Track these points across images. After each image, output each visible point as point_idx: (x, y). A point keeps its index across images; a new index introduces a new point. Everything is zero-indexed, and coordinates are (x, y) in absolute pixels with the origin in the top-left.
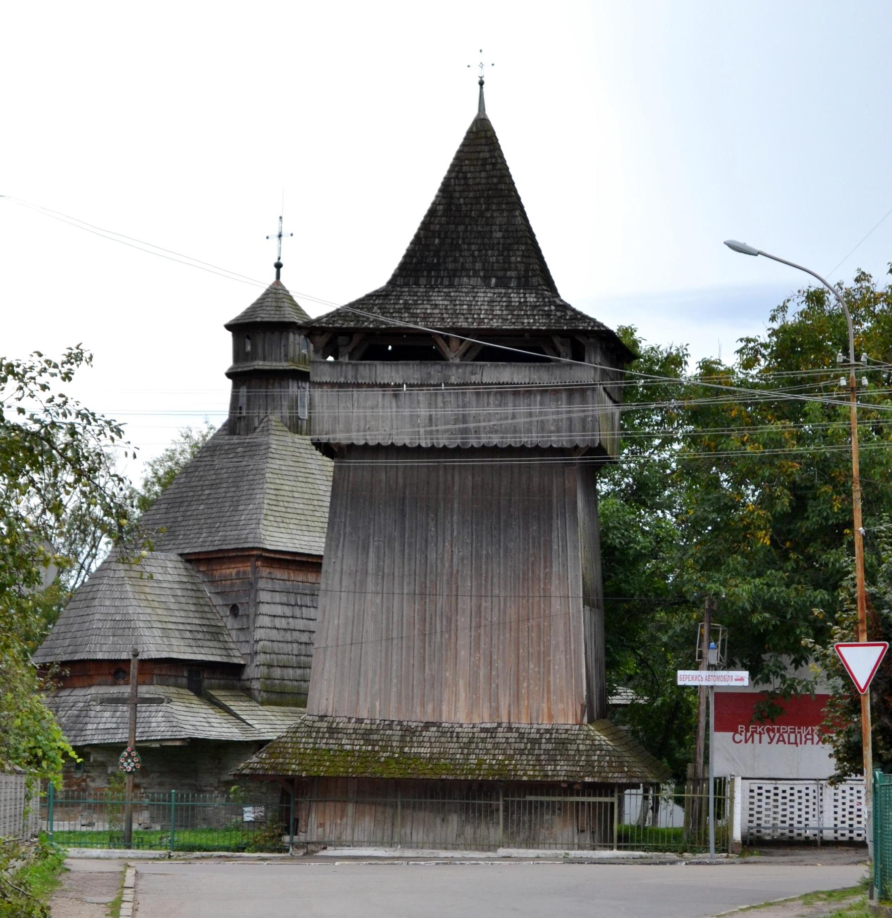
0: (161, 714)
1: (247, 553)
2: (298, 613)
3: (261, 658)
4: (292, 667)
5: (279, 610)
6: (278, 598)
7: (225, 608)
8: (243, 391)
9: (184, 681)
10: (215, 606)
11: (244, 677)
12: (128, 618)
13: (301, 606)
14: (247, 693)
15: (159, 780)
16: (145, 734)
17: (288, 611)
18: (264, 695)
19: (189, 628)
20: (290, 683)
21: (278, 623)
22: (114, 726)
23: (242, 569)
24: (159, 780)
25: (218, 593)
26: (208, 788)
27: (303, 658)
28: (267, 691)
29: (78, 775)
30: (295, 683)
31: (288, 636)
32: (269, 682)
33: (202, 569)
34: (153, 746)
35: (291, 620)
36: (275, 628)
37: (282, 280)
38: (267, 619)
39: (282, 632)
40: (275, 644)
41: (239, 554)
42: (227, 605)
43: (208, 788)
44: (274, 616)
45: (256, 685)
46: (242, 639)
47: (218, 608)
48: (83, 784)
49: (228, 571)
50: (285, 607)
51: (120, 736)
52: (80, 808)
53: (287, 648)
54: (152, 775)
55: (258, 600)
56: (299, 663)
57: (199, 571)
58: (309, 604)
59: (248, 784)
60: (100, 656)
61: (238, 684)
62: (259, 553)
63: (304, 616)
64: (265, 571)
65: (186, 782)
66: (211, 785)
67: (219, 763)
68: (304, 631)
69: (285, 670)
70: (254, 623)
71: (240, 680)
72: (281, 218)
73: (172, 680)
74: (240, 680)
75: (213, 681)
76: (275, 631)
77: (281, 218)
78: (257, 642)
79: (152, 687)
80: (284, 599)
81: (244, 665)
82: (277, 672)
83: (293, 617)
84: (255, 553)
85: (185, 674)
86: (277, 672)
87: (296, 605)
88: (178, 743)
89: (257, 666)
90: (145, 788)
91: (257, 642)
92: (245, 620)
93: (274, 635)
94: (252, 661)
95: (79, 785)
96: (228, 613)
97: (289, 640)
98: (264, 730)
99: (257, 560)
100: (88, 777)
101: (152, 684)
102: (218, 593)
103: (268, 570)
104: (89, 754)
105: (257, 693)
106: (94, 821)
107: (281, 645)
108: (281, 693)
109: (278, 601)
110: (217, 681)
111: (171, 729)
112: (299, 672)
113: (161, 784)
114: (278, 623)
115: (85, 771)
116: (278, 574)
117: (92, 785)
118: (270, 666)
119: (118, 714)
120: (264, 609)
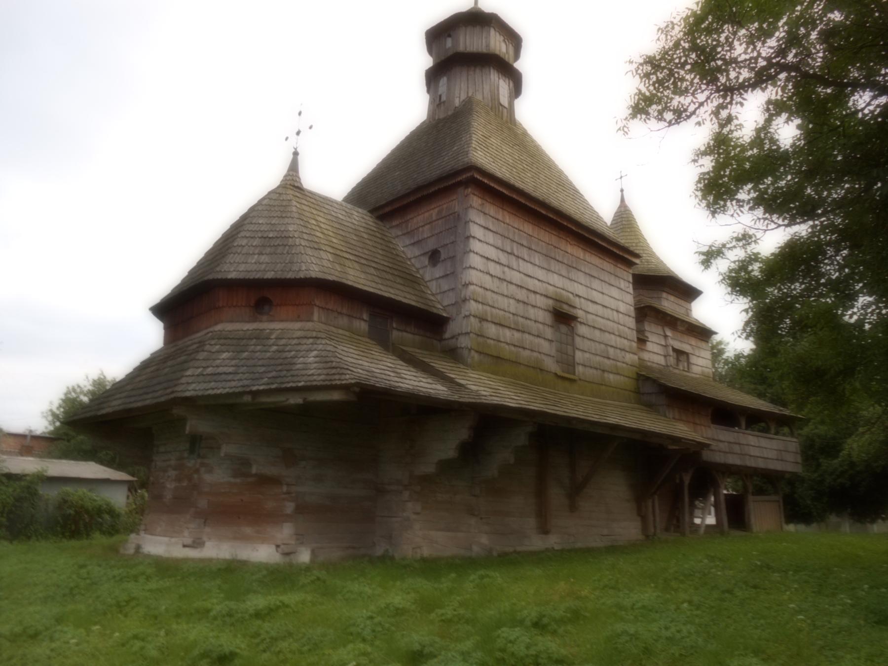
0: (315, 353)
2: (514, 262)
3: (473, 307)
4: (509, 328)
5: (492, 253)
6: (490, 237)
7: (422, 258)
8: (444, 81)
9: (363, 326)
10: (410, 259)
11: (447, 335)
12: (285, 234)
13: (518, 257)
14: (453, 354)
16: (279, 380)
18: (476, 356)
19: (374, 265)
20: (507, 347)
21: (493, 268)
22: (231, 369)
23: (445, 206)
25: (413, 244)
27: (521, 320)
28: (477, 351)
30: (513, 348)
31: (503, 288)
32: (481, 340)
33: (395, 223)
35: (506, 269)
36: (488, 273)
40: (489, 293)
42: (424, 254)
44: (488, 259)
45: (464, 342)
46: (445, 287)
47: (413, 261)
48: (196, 476)
49: (427, 215)
50: (500, 253)
51: (233, 384)
53: (503, 302)
55: (467, 234)
57: (391, 227)
58: (526, 258)
60: (232, 275)
63: (521, 270)
64: (476, 201)
68: (521, 287)
69: (501, 329)
71: (441, 340)
73: (344, 321)
75: (405, 334)
76: (488, 277)
78: (466, 285)
79: (309, 325)
80: (499, 243)
82: (492, 330)
83: (508, 267)
85: (365, 316)
87: (512, 254)
88: (336, 396)
89: (466, 317)
90: (288, 485)
91: (466, 285)
93: (487, 281)
96: (427, 262)
97: (506, 293)
99: (467, 187)
101: (310, 320)
102: (413, 244)
103: (480, 201)
105: (466, 352)
107: (494, 295)
108: (498, 358)
109: (491, 242)
110: (410, 336)
111: (325, 372)
112: (517, 335)
115: (199, 456)
116: (491, 209)
118: (482, 319)
119: (245, 354)
120: (475, 245)
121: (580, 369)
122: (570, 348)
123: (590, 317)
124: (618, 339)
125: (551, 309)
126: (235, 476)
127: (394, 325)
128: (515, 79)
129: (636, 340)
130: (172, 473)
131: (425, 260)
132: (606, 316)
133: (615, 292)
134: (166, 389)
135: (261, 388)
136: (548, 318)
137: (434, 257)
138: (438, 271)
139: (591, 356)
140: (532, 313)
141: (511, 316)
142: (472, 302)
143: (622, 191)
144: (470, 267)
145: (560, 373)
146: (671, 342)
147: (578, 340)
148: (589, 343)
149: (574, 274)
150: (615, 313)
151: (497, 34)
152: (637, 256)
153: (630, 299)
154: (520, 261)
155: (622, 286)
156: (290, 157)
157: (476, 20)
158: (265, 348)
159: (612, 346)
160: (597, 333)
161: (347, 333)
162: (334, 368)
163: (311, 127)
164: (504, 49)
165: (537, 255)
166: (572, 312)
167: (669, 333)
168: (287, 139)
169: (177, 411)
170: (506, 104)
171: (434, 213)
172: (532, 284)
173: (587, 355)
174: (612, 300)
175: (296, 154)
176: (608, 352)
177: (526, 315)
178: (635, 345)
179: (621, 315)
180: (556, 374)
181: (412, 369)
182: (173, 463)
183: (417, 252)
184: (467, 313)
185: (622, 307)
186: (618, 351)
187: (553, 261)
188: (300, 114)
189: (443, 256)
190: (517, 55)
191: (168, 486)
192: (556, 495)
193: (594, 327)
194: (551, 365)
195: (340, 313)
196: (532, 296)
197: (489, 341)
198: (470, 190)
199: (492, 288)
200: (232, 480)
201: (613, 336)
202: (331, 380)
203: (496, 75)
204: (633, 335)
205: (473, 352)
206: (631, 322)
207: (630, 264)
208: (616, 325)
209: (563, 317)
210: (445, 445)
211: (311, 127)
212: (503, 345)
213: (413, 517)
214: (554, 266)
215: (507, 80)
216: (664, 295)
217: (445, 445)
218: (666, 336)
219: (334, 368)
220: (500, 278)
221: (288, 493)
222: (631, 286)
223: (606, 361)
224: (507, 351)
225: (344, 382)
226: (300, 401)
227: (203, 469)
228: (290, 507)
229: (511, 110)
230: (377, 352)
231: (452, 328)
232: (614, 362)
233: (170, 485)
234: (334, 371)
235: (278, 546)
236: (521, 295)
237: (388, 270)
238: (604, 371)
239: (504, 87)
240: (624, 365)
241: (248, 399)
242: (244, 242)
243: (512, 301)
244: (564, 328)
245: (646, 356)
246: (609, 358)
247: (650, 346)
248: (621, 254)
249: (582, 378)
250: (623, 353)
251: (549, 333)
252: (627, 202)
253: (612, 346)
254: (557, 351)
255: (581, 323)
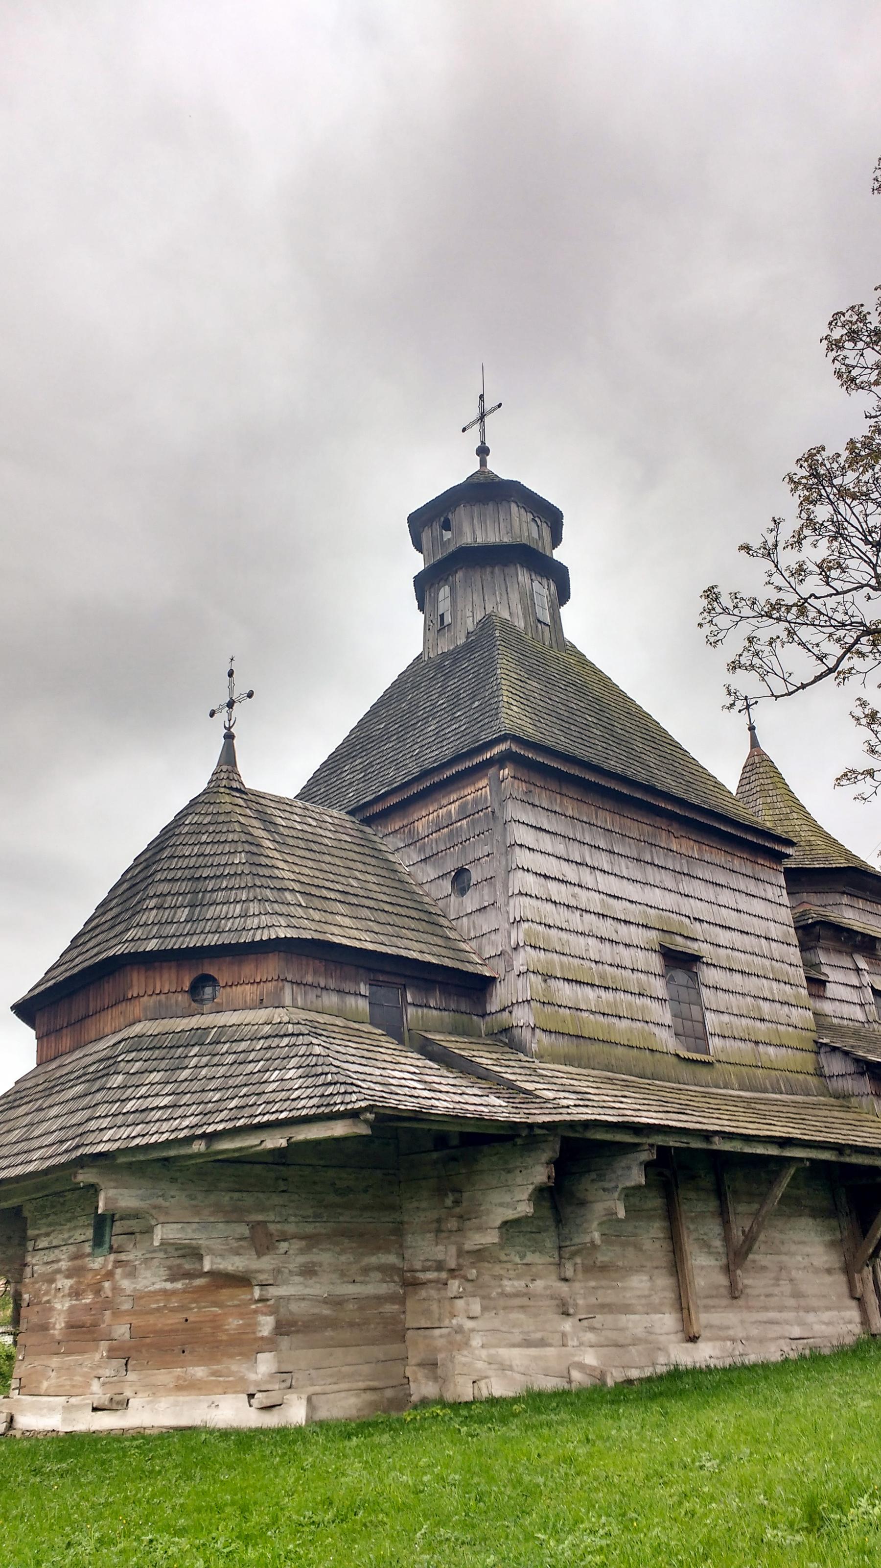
0: (294, 1062)
1: (480, 759)
2: (587, 877)
4: (592, 985)
6: (547, 843)
8: (444, 592)
9: (363, 1005)
11: (493, 1007)
15: (301, 1259)
16: (247, 1112)
17: (570, 872)
18: (545, 1038)
22: (166, 1101)
24: (301, 1259)
26: (431, 1275)
29: (96, 1263)
30: (600, 1018)
32: (549, 1009)
34: (269, 1144)
35: (577, 889)
37: (490, 467)
38: (530, 878)
39: (564, 912)
40: (554, 932)
41: (460, 767)
43: (431, 1275)
44: (546, 877)
45: (522, 1016)
48: (107, 1285)
52: (97, 1356)
53: (579, 944)
54: (284, 1246)
56: (602, 977)
59: (530, 1258)
61: (483, 1025)
62: (503, 747)
65: (373, 1260)
66: (440, 1266)
67: (457, 1202)
70: (506, 886)
72: (482, 397)
73: (331, 1000)
74: (483, 1015)
76: (550, 907)
77: (482, 397)
78: (517, 922)
79: (280, 1015)
81: (493, 980)
82: (566, 992)
83: (580, 886)
84: (496, 750)
86: (566, 992)
88: (339, 1129)
91: (517, 922)
92: (486, 891)
94: (509, 968)
95: (98, 1292)
98: (565, 1102)
100: (118, 1263)
103: (524, 787)
104: (93, 1190)
105: (526, 1034)
106: (128, 1393)
107: (564, 935)
109: (550, 850)
110: (435, 1013)
113: (309, 1271)
114: (556, 890)
115: (111, 1250)
117: (126, 1284)
118: (547, 977)
119: (185, 1074)
121: (715, 1043)
122: (695, 1009)
123: (722, 951)
124: (775, 985)
125: (657, 948)
126: (172, 1279)
127: (410, 1000)
128: (559, 580)
129: (805, 984)
130: (65, 1283)
131: (447, 886)
132: (749, 949)
133: (758, 907)
134: (62, 1142)
135: (220, 1127)
136: (655, 962)
137: (460, 880)
138: (471, 902)
139: (732, 1018)
140: (626, 956)
141: (593, 965)
142: (528, 948)
143: (752, 728)
144: (520, 893)
145: (684, 1054)
146: (867, 979)
147: (705, 993)
148: (726, 996)
149: (687, 886)
150: (763, 940)
151: (522, 511)
152: (790, 843)
153: (785, 915)
154: (598, 873)
155: (770, 896)
156: (220, 742)
157: (486, 491)
158: (216, 1060)
159: (765, 999)
160: (738, 977)
161: (339, 1022)
162: (330, 1084)
163: (250, 695)
164: (535, 535)
165: (623, 861)
166: (693, 948)
167: (862, 964)
168: (212, 714)
169: (84, 1177)
170: (548, 620)
171: (452, 807)
172: (619, 908)
173: (725, 1018)
174: (755, 920)
175: (229, 737)
176: (759, 1008)
177: (617, 961)
178: (804, 992)
179: (773, 944)
180: (677, 1055)
181: (446, 1073)
182: (64, 1265)
183: (431, 872)
184: (523, 969)
185: (775, 931)
186: (778, 1005)
187: (649, 868)
188: (231, 674)
189: (475, 876)
190: (556, 540)
191: (58, 1306)
192: (704, 1267)
193: (731, 970)
194: (666, 1040)
195: (325, 988)
196: (623, 929)
197: (562, 1010)
198: (506, 771)
199: (558, 924)
200: (169, 1286)
201: (764, 981)
202: (328, 1105)
203: (527, 576)
204: (799, 975)
205: (537, 1030)
206: (794, 954)
207: (779, 857)
208: (767, 963)
209: (680, 961)
210: (512, 1196)
211: (250, 695)
212: (585, 1015)
213: (469, 1324)
214: (653, 875)
215: (545, 582)
216: (845, 900)
217: (512, 1196)
218: (858, 970)
219: (330, 1084)
220: (568, 906)
221: (261, 1300)
222: (784, 892)
223: (758, 1024)
224: (593, 1024)
225: (349, 1107)
226: (283, 1143)
227: (119, 1271)
228: (266, 1325)
229: (556, 624)
230: (388, 1047)
231: (500, 995)
232: (774, 1026)
233: (62, 1305)
234: (330, 1090)
235: (251, 1396)
236: (606, 928)
237: (387, 907)
238: (757, 1043)
239: (542, 590)
240: (790, 1029)
241: (199, 1146)
242: (164, 888)
243: (591, 941)
244: (681, 976)
245: (827, 1007)
246: (763, 1020)
247: (832, 990)
248: (761, 842)
249: (723, 1058)
250: (786, 1007)
251: (658, 987)
252: (765, 746)
253: (765, 999)
254: (675, 1015)
255: (707, 964)
